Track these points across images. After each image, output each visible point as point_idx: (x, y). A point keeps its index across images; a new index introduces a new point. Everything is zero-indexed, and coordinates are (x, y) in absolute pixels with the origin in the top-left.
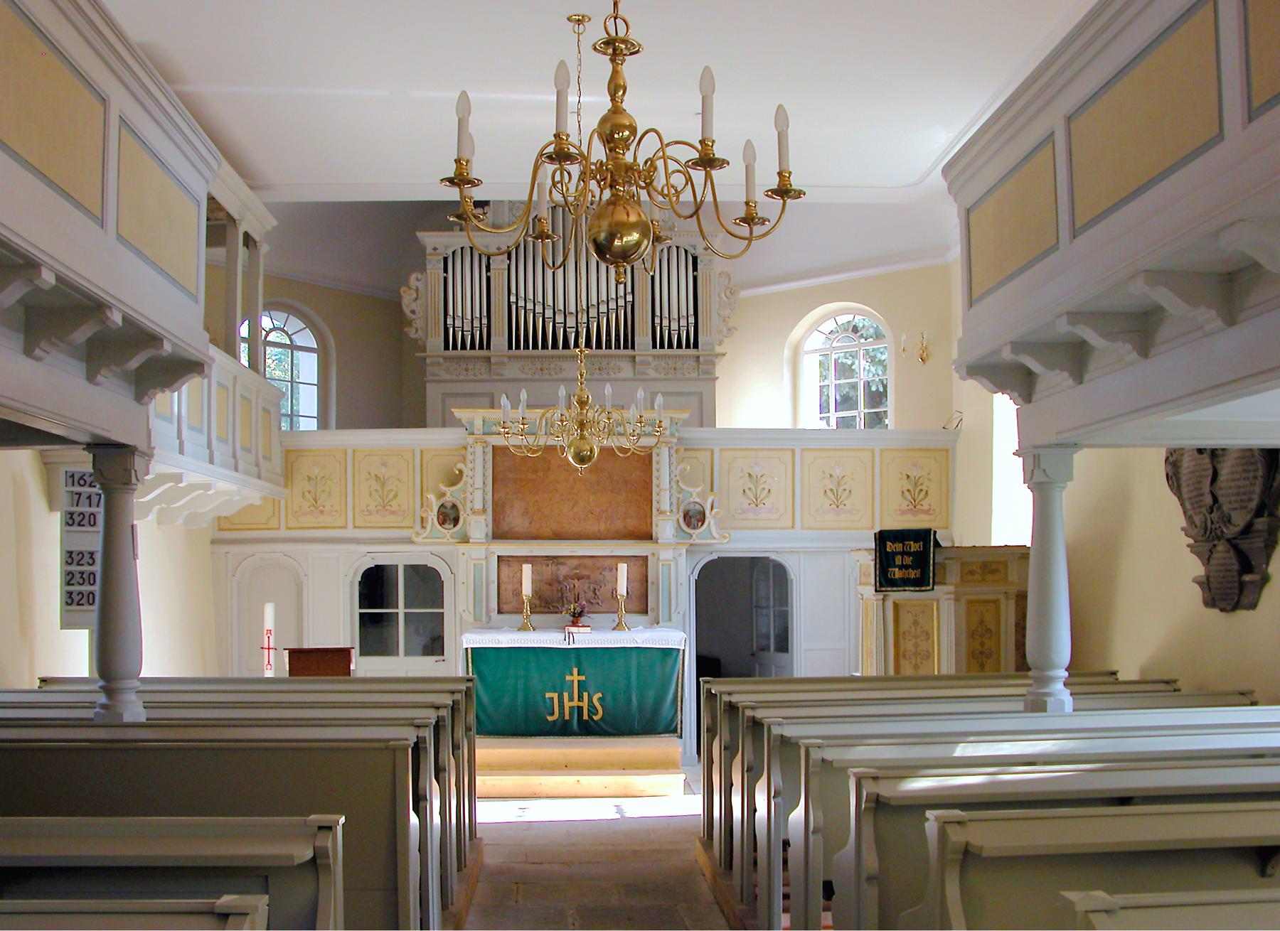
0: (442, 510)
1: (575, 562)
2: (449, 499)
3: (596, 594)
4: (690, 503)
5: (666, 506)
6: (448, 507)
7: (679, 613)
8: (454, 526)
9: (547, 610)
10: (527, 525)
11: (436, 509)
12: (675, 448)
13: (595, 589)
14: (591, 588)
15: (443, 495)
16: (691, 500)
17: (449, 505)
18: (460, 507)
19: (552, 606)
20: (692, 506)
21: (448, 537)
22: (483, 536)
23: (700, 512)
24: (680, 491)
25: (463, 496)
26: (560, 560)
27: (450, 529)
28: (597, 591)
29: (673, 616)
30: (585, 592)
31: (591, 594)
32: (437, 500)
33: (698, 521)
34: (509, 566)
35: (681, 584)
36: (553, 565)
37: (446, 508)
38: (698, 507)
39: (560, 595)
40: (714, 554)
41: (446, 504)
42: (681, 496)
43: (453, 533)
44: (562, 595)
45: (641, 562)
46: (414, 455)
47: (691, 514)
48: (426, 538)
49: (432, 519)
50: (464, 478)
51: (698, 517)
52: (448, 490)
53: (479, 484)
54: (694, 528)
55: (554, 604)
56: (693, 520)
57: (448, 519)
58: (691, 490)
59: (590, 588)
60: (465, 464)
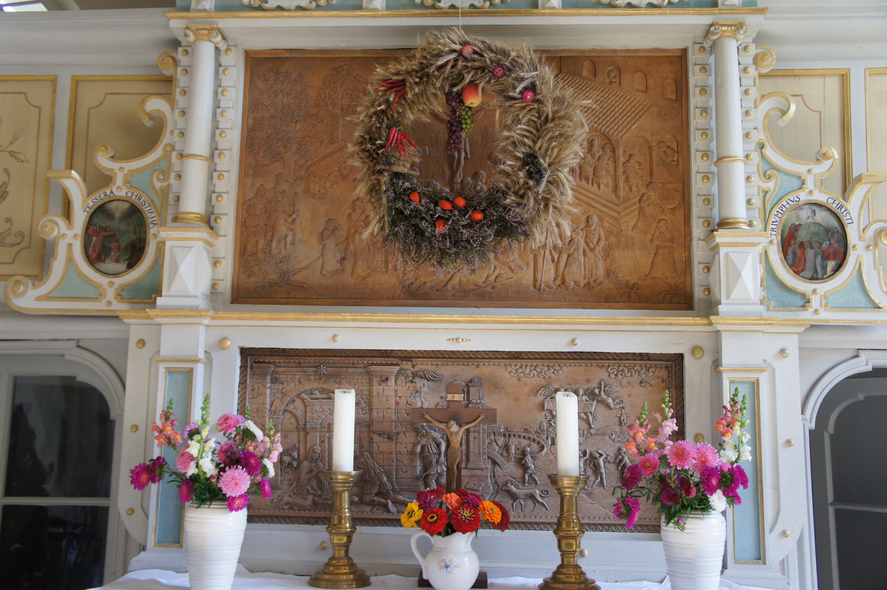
0: (101, 221)
1: (466, 372)
2: (122, 193)
3: (525, 468)
4: (799, 208)
5: (739, 211)
6: (118, 215)
7: (784, 534)
8: (131, 266)
9: (381, 514)
10: (332, 263)
11: (80, 217)
12: (753, 50)
13: (524, 454)
14: (513, 450)
15: (107, 179)
16: (803, 196)
17: (118, 209)
18: (150, 215)
19: (395, 502)
20: (805, 213)
21: (111, 294)
22: (204, 287)
23: (828, 231)
24: (769, 170)
25: (158, 185)
26: (422, 366)
27: (116, 275)
28: (529, 458)
29: (771, 540)
30: (494, 463)
31: (510, 469)
32: (89, 194)
33: (826, 257)
34: (274, 381)
35: (788, 443)
36: (402, 379)
37: (110, 215)
38: (822, 217)
39: (419, 468)
40: (863, 355)
41: (112, 206)
42: (771, 185)
43: (122, 288)
44: (426, 468)
45: (663, 373)
46: (55, 91)
47: (802, 236)
48: (48, 297)
49: (70, 246)
50: (166, 139)
51: (825, 245)
52: (121, 170)
53: (199, 142)
54: (814, 278)
55: (401, 498)
56: (810, 253)
57: (113, 245)
58: (800, 168)
59: (507, 447)
60: (168, 96)
